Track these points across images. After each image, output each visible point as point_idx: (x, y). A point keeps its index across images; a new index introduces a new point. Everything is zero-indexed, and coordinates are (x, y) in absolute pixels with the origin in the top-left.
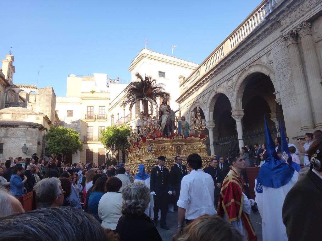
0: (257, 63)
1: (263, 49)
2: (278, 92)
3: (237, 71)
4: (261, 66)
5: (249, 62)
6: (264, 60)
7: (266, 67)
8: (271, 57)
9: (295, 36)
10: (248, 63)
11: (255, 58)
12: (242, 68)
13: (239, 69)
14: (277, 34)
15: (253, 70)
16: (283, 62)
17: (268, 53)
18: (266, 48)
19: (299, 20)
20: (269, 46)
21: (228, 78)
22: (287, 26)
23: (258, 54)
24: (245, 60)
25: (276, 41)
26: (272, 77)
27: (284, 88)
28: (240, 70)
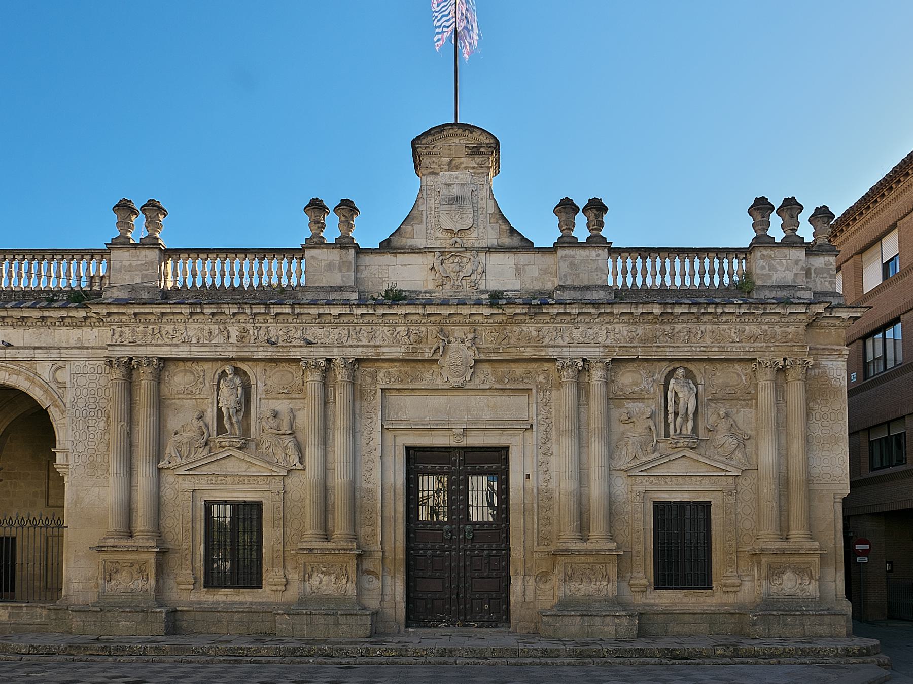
2: (65, 452)
6: (45, 371)
8: (62, 376)
9: (130, 367)
14: (92, 336)
19: (148, 349)
20: (65, 351)
22: (122, 344)
26: (55, 414)
27: (80, 448)
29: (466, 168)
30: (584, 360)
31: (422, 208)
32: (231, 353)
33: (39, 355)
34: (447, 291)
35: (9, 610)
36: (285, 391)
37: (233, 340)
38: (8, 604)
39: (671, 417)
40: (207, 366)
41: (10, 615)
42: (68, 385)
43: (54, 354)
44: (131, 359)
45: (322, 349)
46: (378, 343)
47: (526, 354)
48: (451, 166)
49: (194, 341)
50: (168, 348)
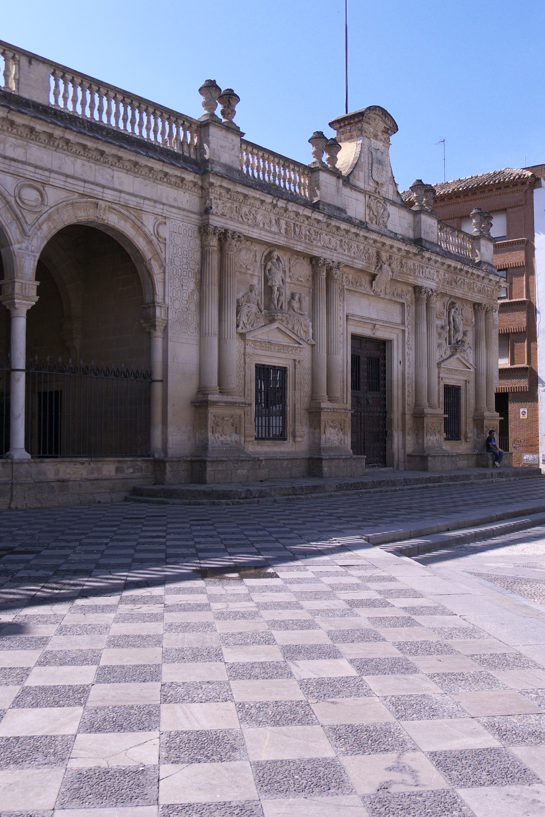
0: (132, 217)
1: (156, 202)
3: (70, 187)
4: (134, 225)
5: (115, 198)
6: (149, 223)
7: (150, 242)
8: (164, 232)
10: (109, 195)
11: (133, 202)
12: (88, 191)
13: (80, 187)
15: (113, 220)
16: (185, 260)
17: (163, 220)
18: (161, 206)
19: (236, 224)
21: (28, 175)
23: (142, 201)
24: (100, 180)
25: (182, 213)
28: (81, 190)
29: (381, 140)
30: (431, 290)
31: (362, 160)
32: (282, 241)
33: (147, 206)
34: (373, 226)
35: (116, 465)
36: (302, 279)
37: (283, 231)
38: (117, 459)
39: (452, 332)
40: (257, 248)
41: (118, 470)
42: (168, 242)
43: (159, 209)
44: (226, 230)
45: (328, 252)
46: (352, 255)
47: (410, 280)
48: (376, 137)
49: (261, 226)
50: (247, 228)
